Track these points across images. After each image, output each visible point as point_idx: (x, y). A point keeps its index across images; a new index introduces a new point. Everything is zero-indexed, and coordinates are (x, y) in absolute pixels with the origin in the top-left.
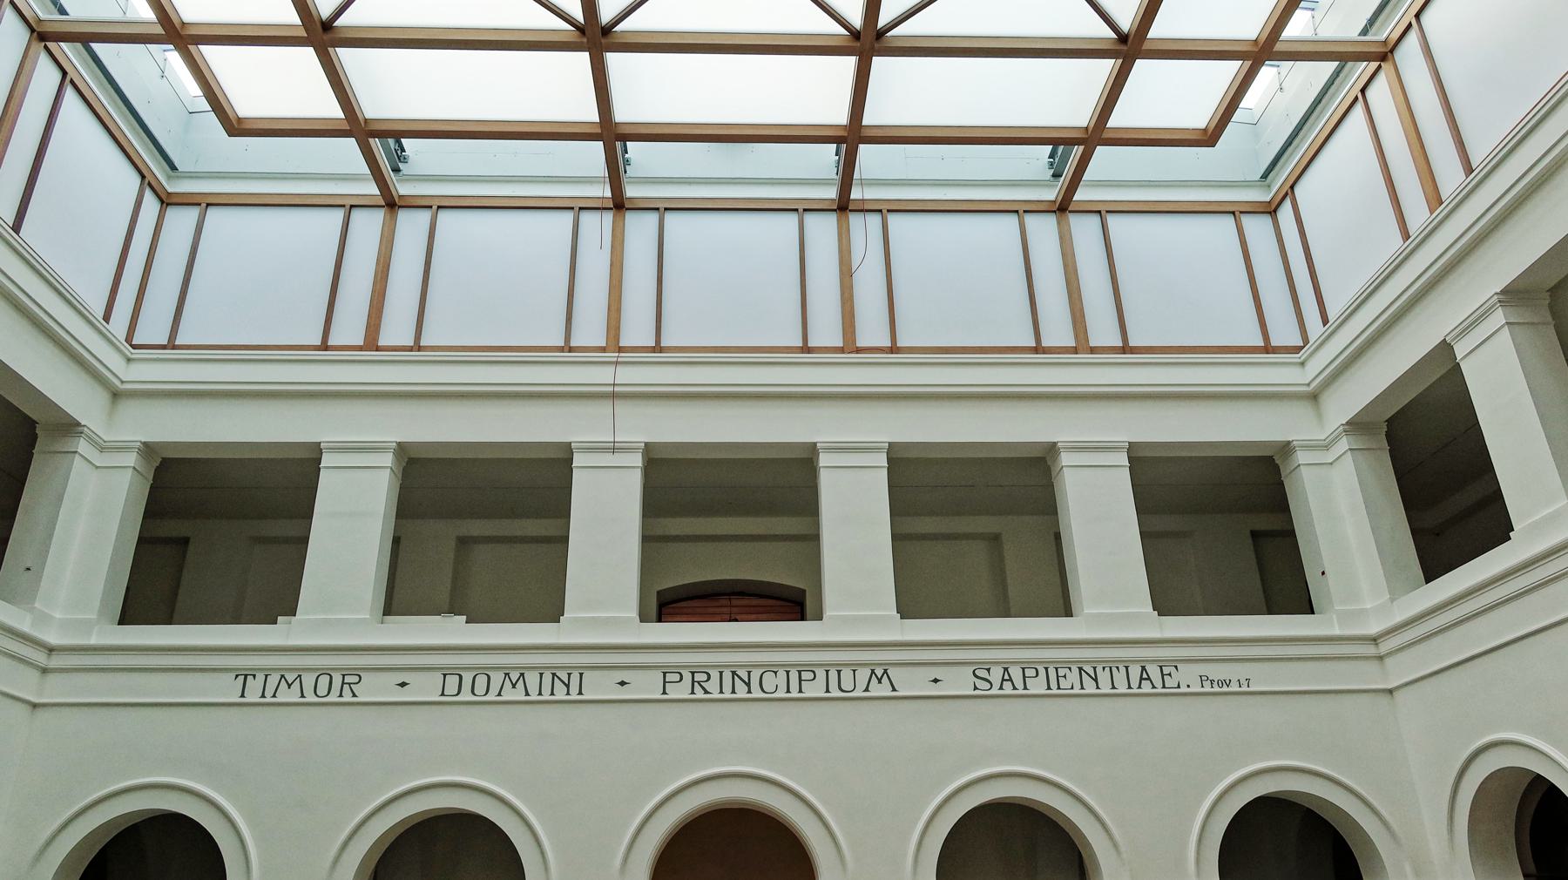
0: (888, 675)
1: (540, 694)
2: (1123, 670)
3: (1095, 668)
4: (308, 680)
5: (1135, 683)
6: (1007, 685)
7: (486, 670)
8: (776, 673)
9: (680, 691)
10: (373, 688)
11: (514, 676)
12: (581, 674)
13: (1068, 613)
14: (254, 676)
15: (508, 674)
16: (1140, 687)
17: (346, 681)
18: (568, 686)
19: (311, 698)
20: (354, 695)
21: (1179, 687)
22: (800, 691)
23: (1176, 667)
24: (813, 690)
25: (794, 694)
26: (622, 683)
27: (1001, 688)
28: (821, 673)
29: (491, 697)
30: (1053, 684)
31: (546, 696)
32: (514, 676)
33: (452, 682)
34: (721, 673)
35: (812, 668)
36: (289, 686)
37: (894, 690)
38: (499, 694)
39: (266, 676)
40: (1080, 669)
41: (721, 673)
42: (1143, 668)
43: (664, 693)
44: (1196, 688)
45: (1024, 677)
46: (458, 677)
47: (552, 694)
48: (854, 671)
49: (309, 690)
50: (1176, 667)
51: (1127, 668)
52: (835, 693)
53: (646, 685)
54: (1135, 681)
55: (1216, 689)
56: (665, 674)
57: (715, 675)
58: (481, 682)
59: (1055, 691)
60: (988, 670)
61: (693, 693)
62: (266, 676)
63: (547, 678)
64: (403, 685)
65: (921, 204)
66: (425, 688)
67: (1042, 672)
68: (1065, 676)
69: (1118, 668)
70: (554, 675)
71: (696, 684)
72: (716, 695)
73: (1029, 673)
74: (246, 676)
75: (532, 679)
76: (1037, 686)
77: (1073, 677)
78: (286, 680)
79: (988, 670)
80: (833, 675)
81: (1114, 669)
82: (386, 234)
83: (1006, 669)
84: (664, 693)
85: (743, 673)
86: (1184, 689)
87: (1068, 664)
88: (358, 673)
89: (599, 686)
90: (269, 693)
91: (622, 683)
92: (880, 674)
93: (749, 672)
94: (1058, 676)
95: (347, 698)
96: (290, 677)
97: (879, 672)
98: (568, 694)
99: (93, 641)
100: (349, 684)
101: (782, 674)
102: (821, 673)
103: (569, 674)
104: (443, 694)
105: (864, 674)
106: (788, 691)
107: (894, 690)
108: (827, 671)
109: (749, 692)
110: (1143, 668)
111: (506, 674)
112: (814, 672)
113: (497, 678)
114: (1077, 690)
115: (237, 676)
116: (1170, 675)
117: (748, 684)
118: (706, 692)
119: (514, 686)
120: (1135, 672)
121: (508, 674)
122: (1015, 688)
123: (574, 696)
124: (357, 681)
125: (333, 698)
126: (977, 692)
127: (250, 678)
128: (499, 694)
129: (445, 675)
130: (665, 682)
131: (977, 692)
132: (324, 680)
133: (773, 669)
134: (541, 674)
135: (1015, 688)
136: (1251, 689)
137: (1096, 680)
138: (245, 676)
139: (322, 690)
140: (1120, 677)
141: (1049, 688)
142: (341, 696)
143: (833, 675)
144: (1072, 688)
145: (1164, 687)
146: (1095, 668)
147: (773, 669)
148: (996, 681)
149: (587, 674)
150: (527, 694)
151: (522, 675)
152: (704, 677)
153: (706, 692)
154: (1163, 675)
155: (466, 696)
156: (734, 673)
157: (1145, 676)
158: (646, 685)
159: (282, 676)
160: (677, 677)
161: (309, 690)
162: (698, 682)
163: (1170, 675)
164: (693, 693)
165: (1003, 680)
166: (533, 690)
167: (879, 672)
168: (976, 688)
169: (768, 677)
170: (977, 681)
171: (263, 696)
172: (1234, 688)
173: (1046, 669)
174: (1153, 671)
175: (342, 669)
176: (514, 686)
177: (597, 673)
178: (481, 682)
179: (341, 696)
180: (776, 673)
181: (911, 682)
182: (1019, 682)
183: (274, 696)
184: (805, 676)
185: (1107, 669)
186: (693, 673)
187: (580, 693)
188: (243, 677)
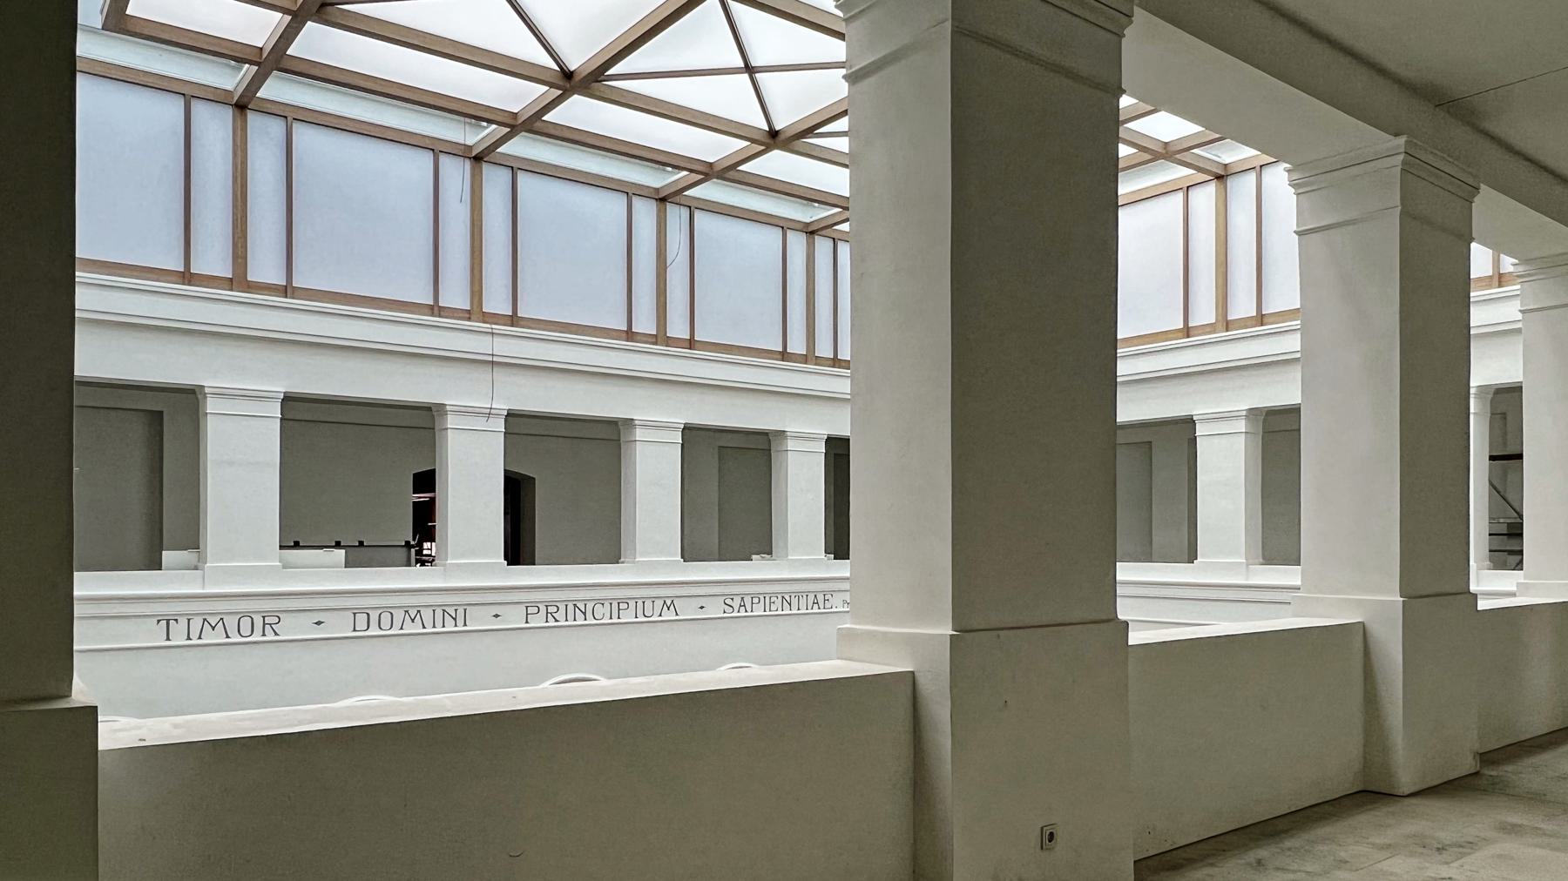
1: (434, 627)
2: (805, 597)
4: (231, 622)
7: (390, 610)
10: (291, 629)
11: (413, 613)
18: (455, 619)
24: (627, 617)
25: (615, 620)
26: (497, 616)
28: (632, 603)
32: (413, 613)
33: (362, 619)
36: (213, 628)
37: (677, 614)
38: (401, 628)
39: (189, 620)
43: (527, 622)
49: (232, 630)
53: (514, 618)
56: (527, 607)
58: (386, 618)
59: (768, 613)
60: (732, 599)
61: (547, 621)
62: (189, 620)
63: (439, 612)
64: (319, 623)
65: (788, 187)
66: (339, 626)
67: (762, 599)
71: (549, 615)
72: (563, 623)
73: (756, 600)
74: (168, 621)
75: (427, 615)
82: (239, 144)
83: (742, 598)
84: (527, 622)
86: (834, 610)
87: (776, 594)
90: (195, 634)
91: (497, 616)
95: (270, 637)
97: (669, 602)
98: (456, 626)
100: (270, 624)
101: (607, 604)
102: (632, 603)
103: (456, 610)
104: (355, 630)
105: (659, 603)
107: (677, 614)
114: (780, 612)
115: (159, 621)
117: (585, 614)
118: (556, 621)
119: (413, 621)
120: (811, 597)
122: (746, 611)
125: (256, 637)
126: (725, 615)
129: (355, 614)
131: (725, 615)
132: (246, 622)
135: (746, 611)
139: (246, 629)
140: (803, 601)
148: (736, 604)
151: (419, 611)
153: (556, 621)
155: (374, 631)
156: (575, 605)
158: (514, 618)
159: (205, 620)
160: (536, 610)
161: (232, 630)
164: (547, 621)
165: (740, 606)
166: (429, 623)
167: (669, 602)
168: (725, 612)
174: (820, 598)
176: (413, 621)
178: (386, 618)
181: (688, 611)
182: (749, 609)
184: (622, 606)
187: (465, 625)
188: (165, 622)
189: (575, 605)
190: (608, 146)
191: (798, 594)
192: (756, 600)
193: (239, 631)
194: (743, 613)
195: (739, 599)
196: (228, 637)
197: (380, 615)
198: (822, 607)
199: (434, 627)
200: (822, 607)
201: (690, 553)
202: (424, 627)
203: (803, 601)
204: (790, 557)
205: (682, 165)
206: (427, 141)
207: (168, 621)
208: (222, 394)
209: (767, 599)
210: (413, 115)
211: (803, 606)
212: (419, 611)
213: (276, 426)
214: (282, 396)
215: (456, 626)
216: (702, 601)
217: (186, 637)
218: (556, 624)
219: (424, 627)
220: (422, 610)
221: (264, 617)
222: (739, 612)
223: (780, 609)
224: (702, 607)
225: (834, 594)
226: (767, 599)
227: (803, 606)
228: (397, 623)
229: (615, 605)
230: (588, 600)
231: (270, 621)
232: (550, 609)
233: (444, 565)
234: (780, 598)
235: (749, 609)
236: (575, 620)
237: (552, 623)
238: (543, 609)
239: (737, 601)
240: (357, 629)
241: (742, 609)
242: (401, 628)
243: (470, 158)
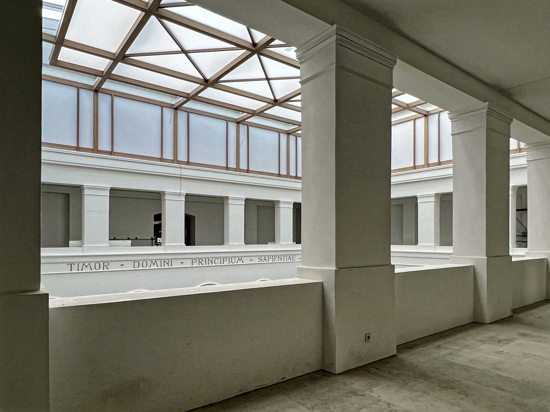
1: (161, 266)
2: (286, 256)
4: (92, 265)
6: (265, 260)
7: (146, 261)
15: (152, 261)
17: (104, 265)
18: (168, 264)
20: (108, 269)
26: (182, 263)
27: (264, 261)
28: (228, 259)
31: (163, 267)
33: (137, 264)
35: (226, 258)
36: (86, 267)
37: (243, 262)
39: (78, 264)
43: (192, 265)
53: (188, 263)
57: (204, 260)
58: (145, 263)
59: (273, 262)
61: (199, 265)
62: (78, 264)
63: (163, 261)
64: (122, 265)
70: (164, 261)
73: (269, 258)
74: (71, 264)
75: (159, 262)
76: (270, 261)
84: (192, 265)
85: (210, 259)
86: (296, 261)
87: (276, 256)
89: (177, 264)
90: (80, 269)
92: (240, 259)
95: (106, 270)
97: (240, 258)
98: (168, 266)
100: (106, 266)
101: (219, 259)
102: (228, 259)
103: (168, 261)
104: (134, 267)
105: (237, 259)
107: (243, 262)
109: (212, 264)
111: (152, 261)
113: (149, 262)
114: (277, 262)
115: (68, 264)
119: (154, 264)
121: (152, 261)
122: (266, 261)
125: (101, 270)
128: (150, 267)
129: (134, 262)
132: (97, 265)
133: (217, 258)
134: (161, 261)
135: (266, 261)
140: (285, 258)
142: (104, 269)
147: (217, 258)
151: (156, 261)
152: (202, 260)
153: (202, 264)
156: (209, 259)
158: (188, 263)
159: (84, 264)
164: (199, 265)
166: (159, 265)
167: (240, 258)
168: (259, 262)
176: (154, 264)
177: (175, 260)
178: (145, 263)
179: (104, 269)
181: (246, 261)
182: (267, 261)
183: (82, 270)
186: (199, 260)
189: (209, 259)
190: (225, 106)
191: (284, 256)
192: (269, 258)
194: (265, 262)
195: (264, 257)
196: (91, 270)
198: (292, 260)
199: (161, 266)
200: (292, 260)
201: (247, 242)
202: (158, 267)
205: (296, 124)
206: (261, 126)
207: (71, 264)
208: (91, 188)
209: (273, 257)
210: (158, 95)
211: (285, 259)
213: (183, 204)
214: (185, 194)
215: (168, 266)
216: (251, 258)
219: (158, 267)
220: (157, 261)
221: (104, 263)
224: (251, 260)
226: (273, 257)
227: (285, 259)
229: (222, 259)
230: (233, 257)
231: (106, 264)
232: (200, 260)
233: (229, 245)
234: (278, 256)
235: (267, 261)
236: (221, 264)
239: (263, 258)
240: (135, 267)
241: (290, 259)
242: (150, 267)
243: (236, 123)
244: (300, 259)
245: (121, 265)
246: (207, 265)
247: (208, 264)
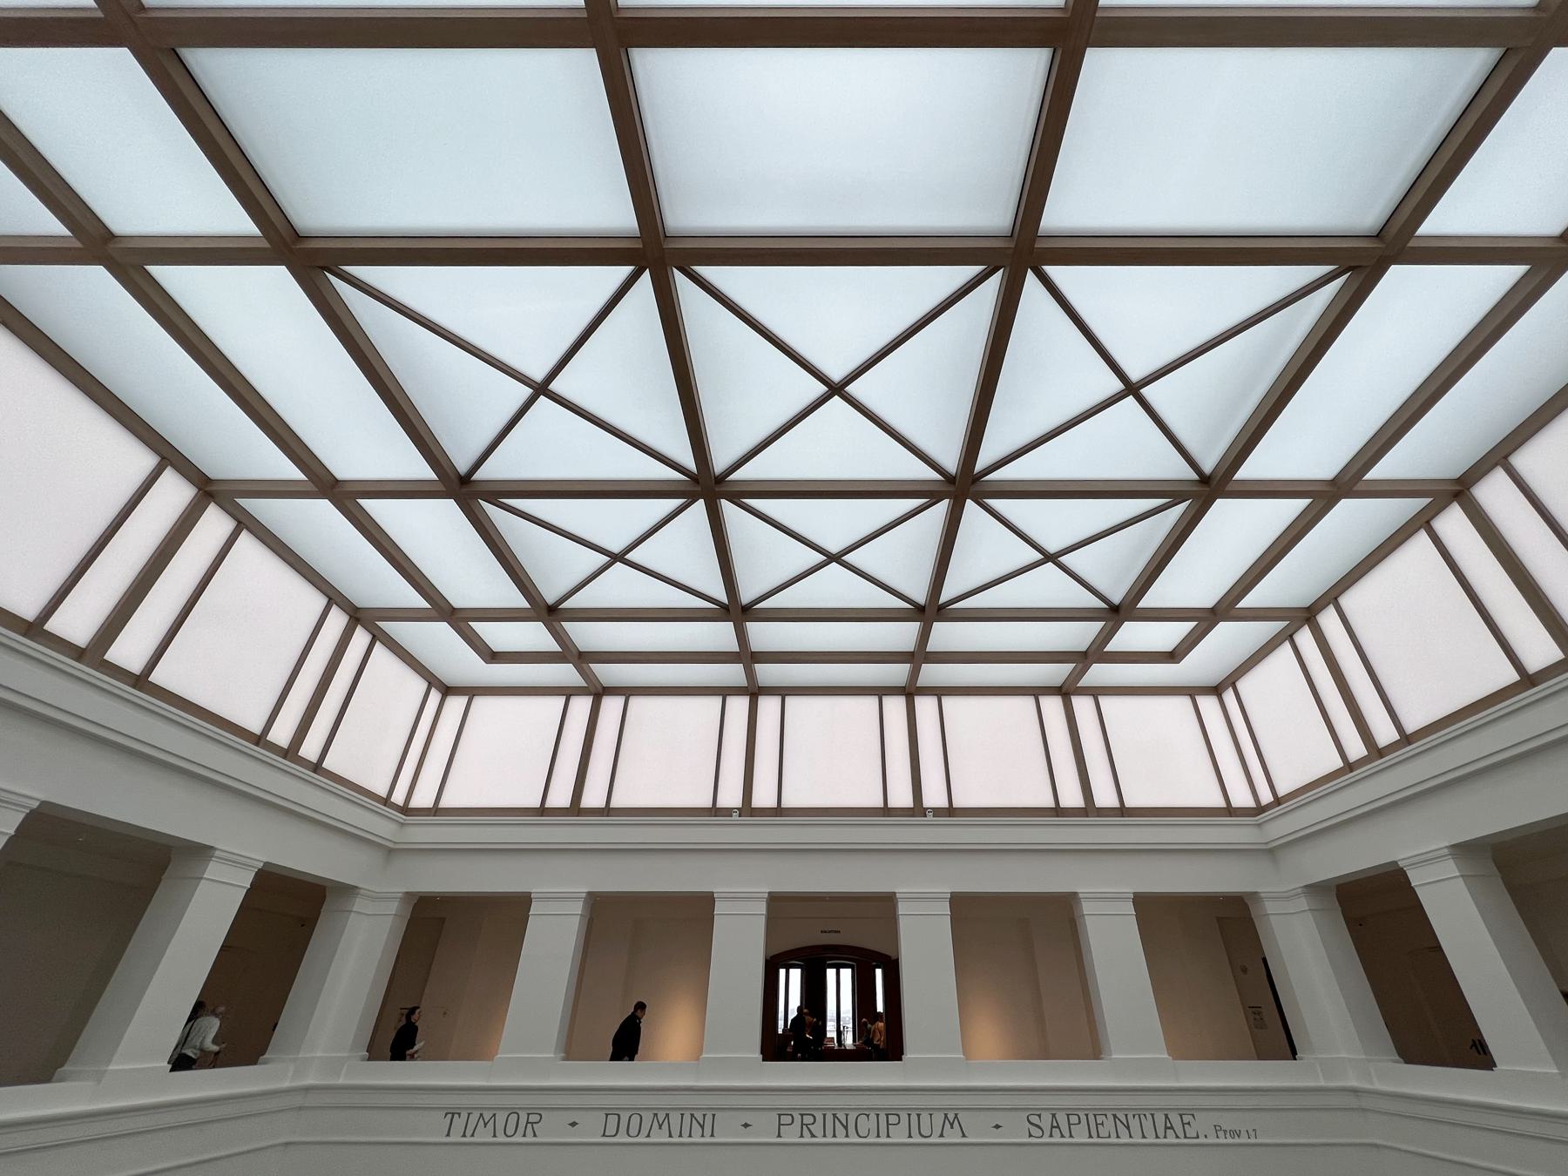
0: (958, 1120)
3: (1126, 1115)
5: (1161, 1132)
7: (637, 1111)
8: (868, 1116)
9: (792, 1134)
10: (552, 1129)
11: (661, 1117)
12: (714, 1115)
13: (1097, 1058)
14: (459, 1114)
16: (1165, 1137)
19: (501, 1139)
21: (1198, 1137)
22: (888, 1136)
23: (1193, 1115)
24: (898, 1136)
25: (883, 1140)
26: (746, 1125)
29: (641, 1139)
30: (1094, 1133)
32: (661, 1117)
33: (613, 1120)
34: (824, 1115)
39: (469, 1114)
40: (1115, 1116)
41: (824, 1115)
42: (1166, 1116)
43: (779, 1136)
44: (1212, 1140)
45: (1069, 1124)
46: (616, 1117)
47: (690, 1136)
48: (931, 1115)
50: (1193, 1115)
51: (1152, 1115)
52: (917, 1139)
54: (1161, 1132)
55: (1230, 1140)
58: (635, 1120)
60: (1039, 1116)
61: (802, 1136)
62: (469, 1114)
64: (573, 1124)
68: (1102, 1124)
69: (1145, 1115)
74: (453, 1114)
75: (675, 1118)
77: (1109, 1123)
78: (483, 1119)
79: (1039, 1116)
80: (914, 1118)
81: (1142, 1116)
83: (1054, 1115)
84: (779, 1136)
86: (1202, 1140)
88: (539, 1112)
90: (469, 1133)
92: (952, 1120)
93: (847, 1115)
94: (1097, 1124)
95: (529, 1139)
96: (487, 1116)
97: (951, 1117)
98: (703, 1136)
99: (341, 1081)
100: (532, 1123)
101: (873, 1116)
103: (704, 1115)
104: (604, 1135)
105: (938, 1118)
106: (878, 1136)
107: (964, 1136)
108: (909, 1115)
109: (847, 1136)
110: (1166, 1116)
111: (656, 1115)
112: (898, 1115)
113: (648, 1117)
114: (1113, 1140)
115: (446, 1114)
116: (1189, 1123)
117: (846, 1128)
118: (813, 1136)
122: (1062, 1136)
123: (708, 1139)
124: (538, 1120)
127: (456, 1116)
129: (607, 1115)
130: (780, 1124)
134: (682, 1115)
136: (1259, 1141)
137: (1128, 1128)
138: (453, 1114)
141: (1090, 1136)
142: (524, 1136)
143: (914, 1118)
144: (1109, 1137)
145: (1185, 1137)
146: (1126, 1115)
149: (719, 1115)
150: (670, 1136)
151: (667, 1115)
153: (813, 1136)
154: (1183, 1124)
157: (1169, 1125)
159: (481, 1115)
162: (806, 1125)
163: (1189, 1123)
164: (802, 1136)
165: (1052, 1127)
166: (675, 1132)
167: (951, 1117)
168: (1030, 1136)
169: (862, 1119)
170: (1030, 1126)
171: (464, 1136)
172: (1244, 1140)
173: (1087, 1115)
174: (1175, 1119)
175: (527, 1108)
180: (868, 1116)
183: (473, 1135)
185: (1137, 1117)
186: (802, 1115)
187: (712, 1135)
191: (1140, 1114)
192: (1074, 1119)
193: (505, 1133)
194: (1057, 1139)
197: (630, 1117)
203: (1148, 1124)
204: (1114, 1056)
209: (1091, 1118)
212: (667, 1115)
216: (998, 1118)
217: (462, 1134)
218: (814, 1140)
222: (1051, 1136)
223: (1114, 1134)
225: (1195, 1114)
226: (1091, 1118)
228: (645, 1131)
232: (806, 1120)
234: (1111, 1118)
237: (807, 1139)
238: (798, 1118)
239: (1046, 1121)
244: (1221, 1134)
245: (570, 1124)
246: (830, 1140)
247: (834, 1136)
